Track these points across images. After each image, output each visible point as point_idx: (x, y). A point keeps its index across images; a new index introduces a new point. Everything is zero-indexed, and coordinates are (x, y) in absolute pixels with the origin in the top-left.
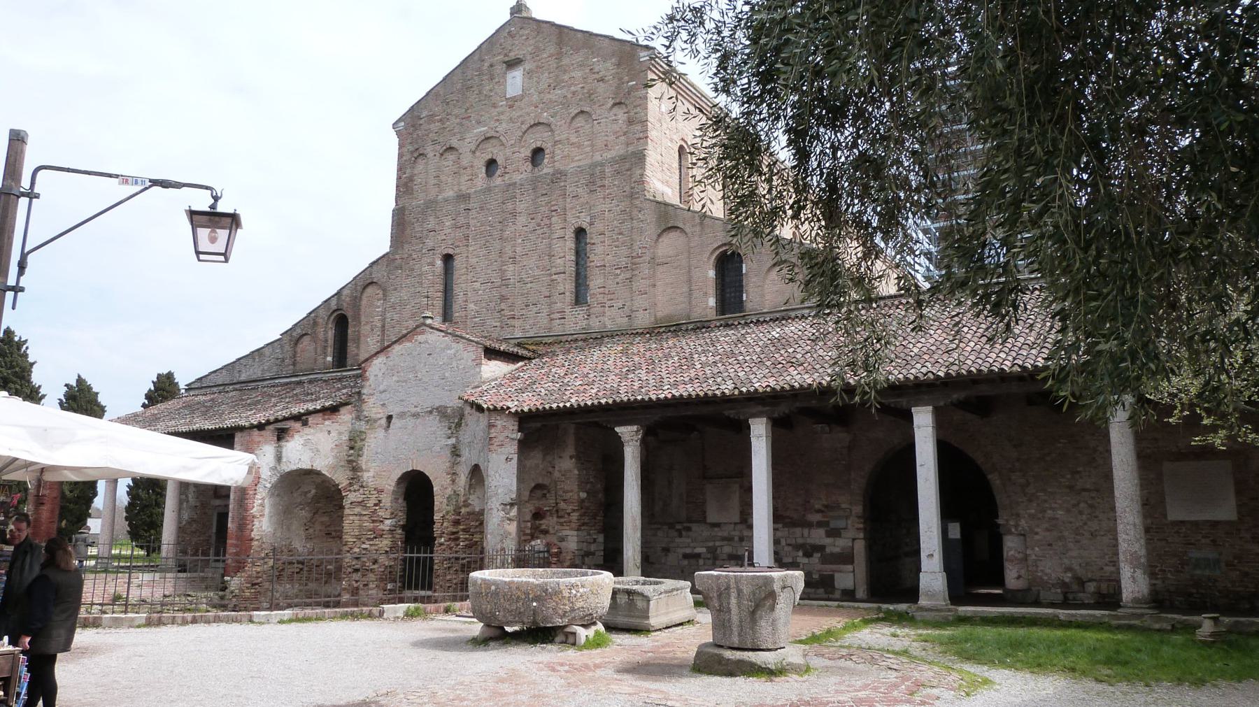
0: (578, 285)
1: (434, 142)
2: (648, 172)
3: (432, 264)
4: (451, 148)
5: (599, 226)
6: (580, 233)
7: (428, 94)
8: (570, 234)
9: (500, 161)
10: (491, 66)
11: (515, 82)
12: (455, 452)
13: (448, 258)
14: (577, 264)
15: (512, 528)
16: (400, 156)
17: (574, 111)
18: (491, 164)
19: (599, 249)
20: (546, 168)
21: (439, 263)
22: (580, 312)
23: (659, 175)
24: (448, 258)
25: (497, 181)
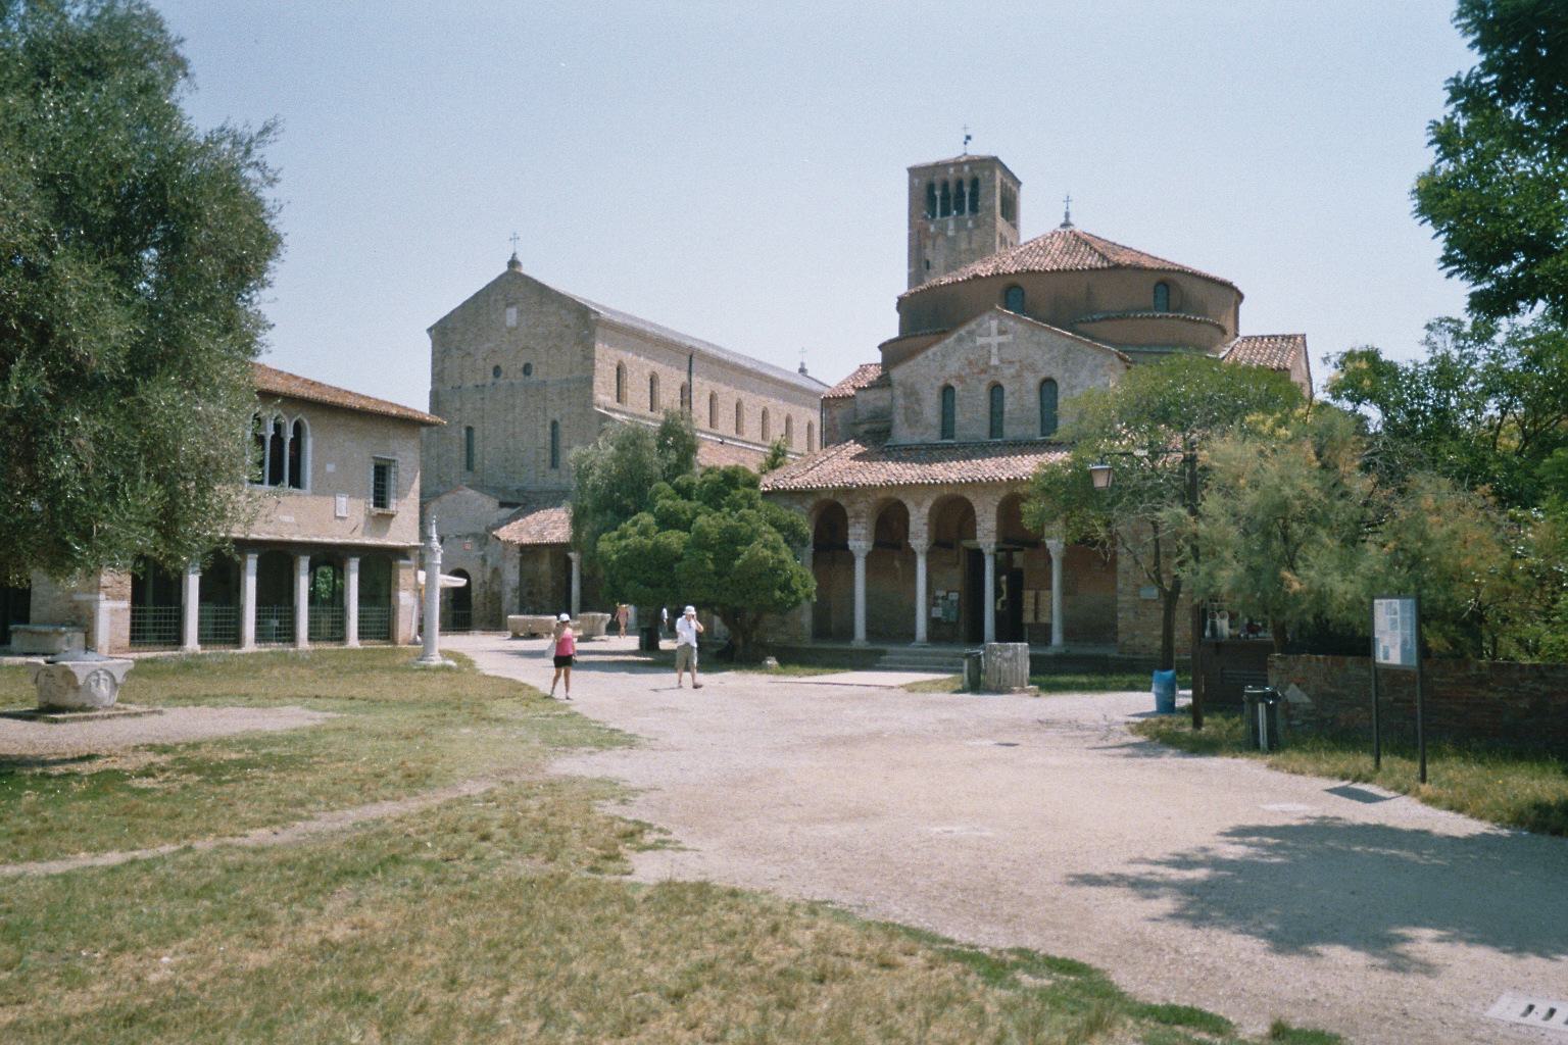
0: (553, 456)
1: (458, 348)
2: (595, 392)
3: (460, 432)
4: (469, 354)
5: (566, 422)
6: (554, 424)
7: (453, 312)
8: (549, 423)
9: (503, 368)
10: (496, 300)
11: (512, 316)
12: (484, 559)
13: (469, 430)
14: (553, 442)
15: (517, 601)
16: (433, 354)
17: (550, 344)
18: (497, 371)
19: (566, 436)
20: (534, 377)
21: (464, 432)
22: (555, 473)
23: (603, 391)
24: (469, 430)
25: (501, 381)
